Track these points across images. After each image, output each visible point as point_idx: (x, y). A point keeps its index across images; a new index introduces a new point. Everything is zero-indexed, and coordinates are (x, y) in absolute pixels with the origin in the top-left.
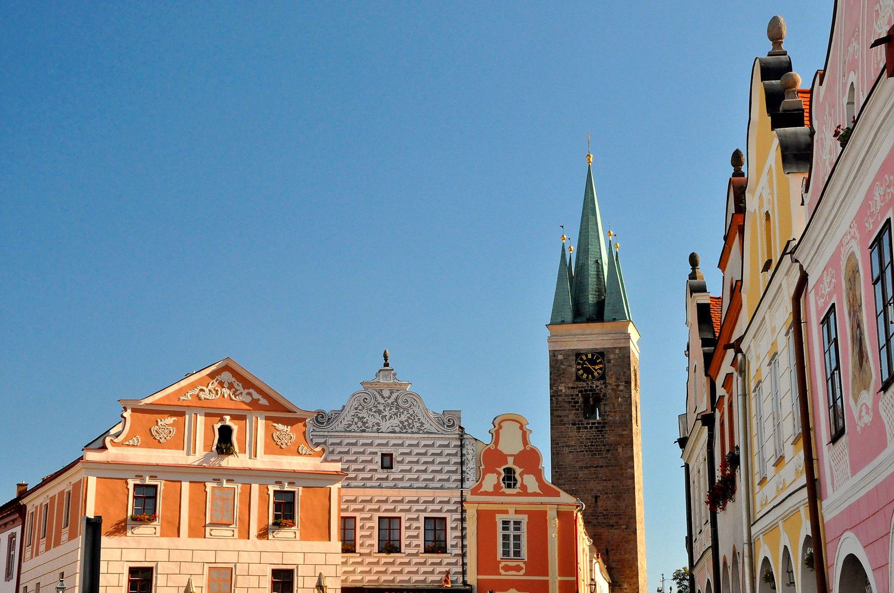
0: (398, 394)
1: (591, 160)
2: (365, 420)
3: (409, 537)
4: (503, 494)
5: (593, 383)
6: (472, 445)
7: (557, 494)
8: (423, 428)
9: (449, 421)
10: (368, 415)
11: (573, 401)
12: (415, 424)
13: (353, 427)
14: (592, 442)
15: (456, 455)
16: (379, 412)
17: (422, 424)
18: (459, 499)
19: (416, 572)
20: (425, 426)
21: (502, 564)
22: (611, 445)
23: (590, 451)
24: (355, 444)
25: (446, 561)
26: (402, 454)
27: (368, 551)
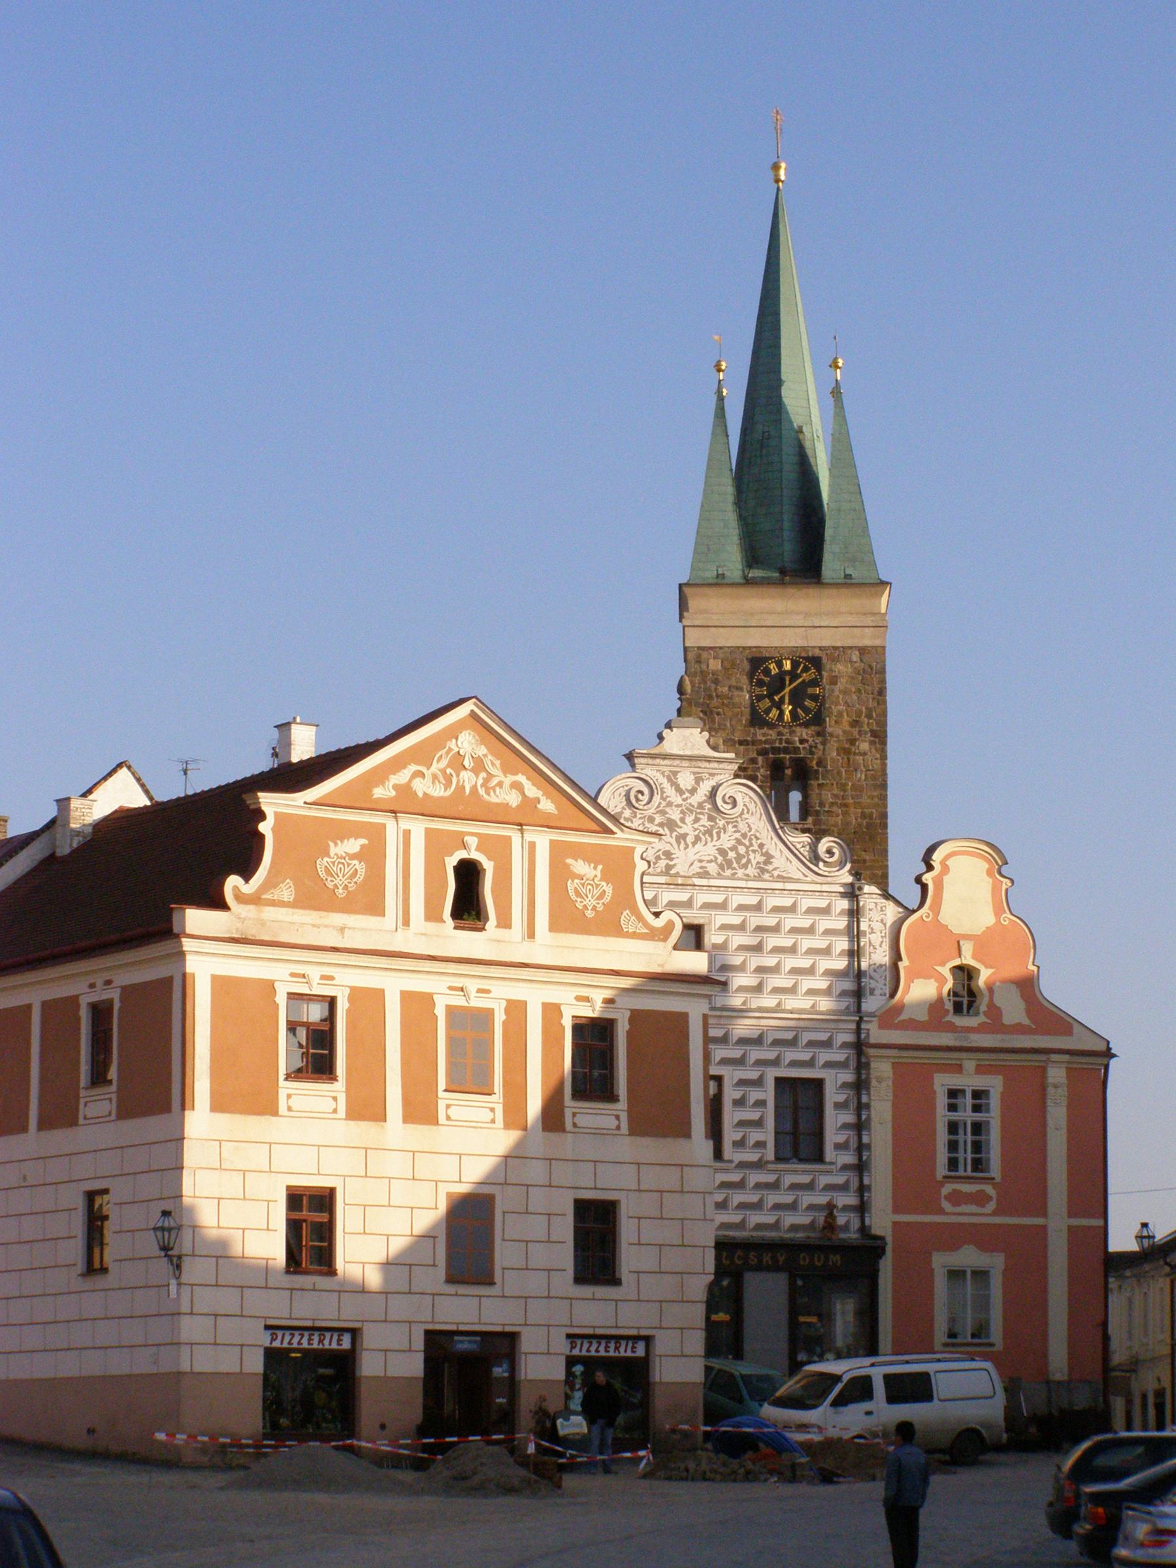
1: (783, 177)
3: (742, 1123)
4: (952, 1028)
6: (882, 911)
8: (770, 868)
12: (752, 856)
16: (671, 825)
17: (769, 858)
20: (776, 863)
21: (947, 1189)
25: (823, 1180)
26: (724, 927)
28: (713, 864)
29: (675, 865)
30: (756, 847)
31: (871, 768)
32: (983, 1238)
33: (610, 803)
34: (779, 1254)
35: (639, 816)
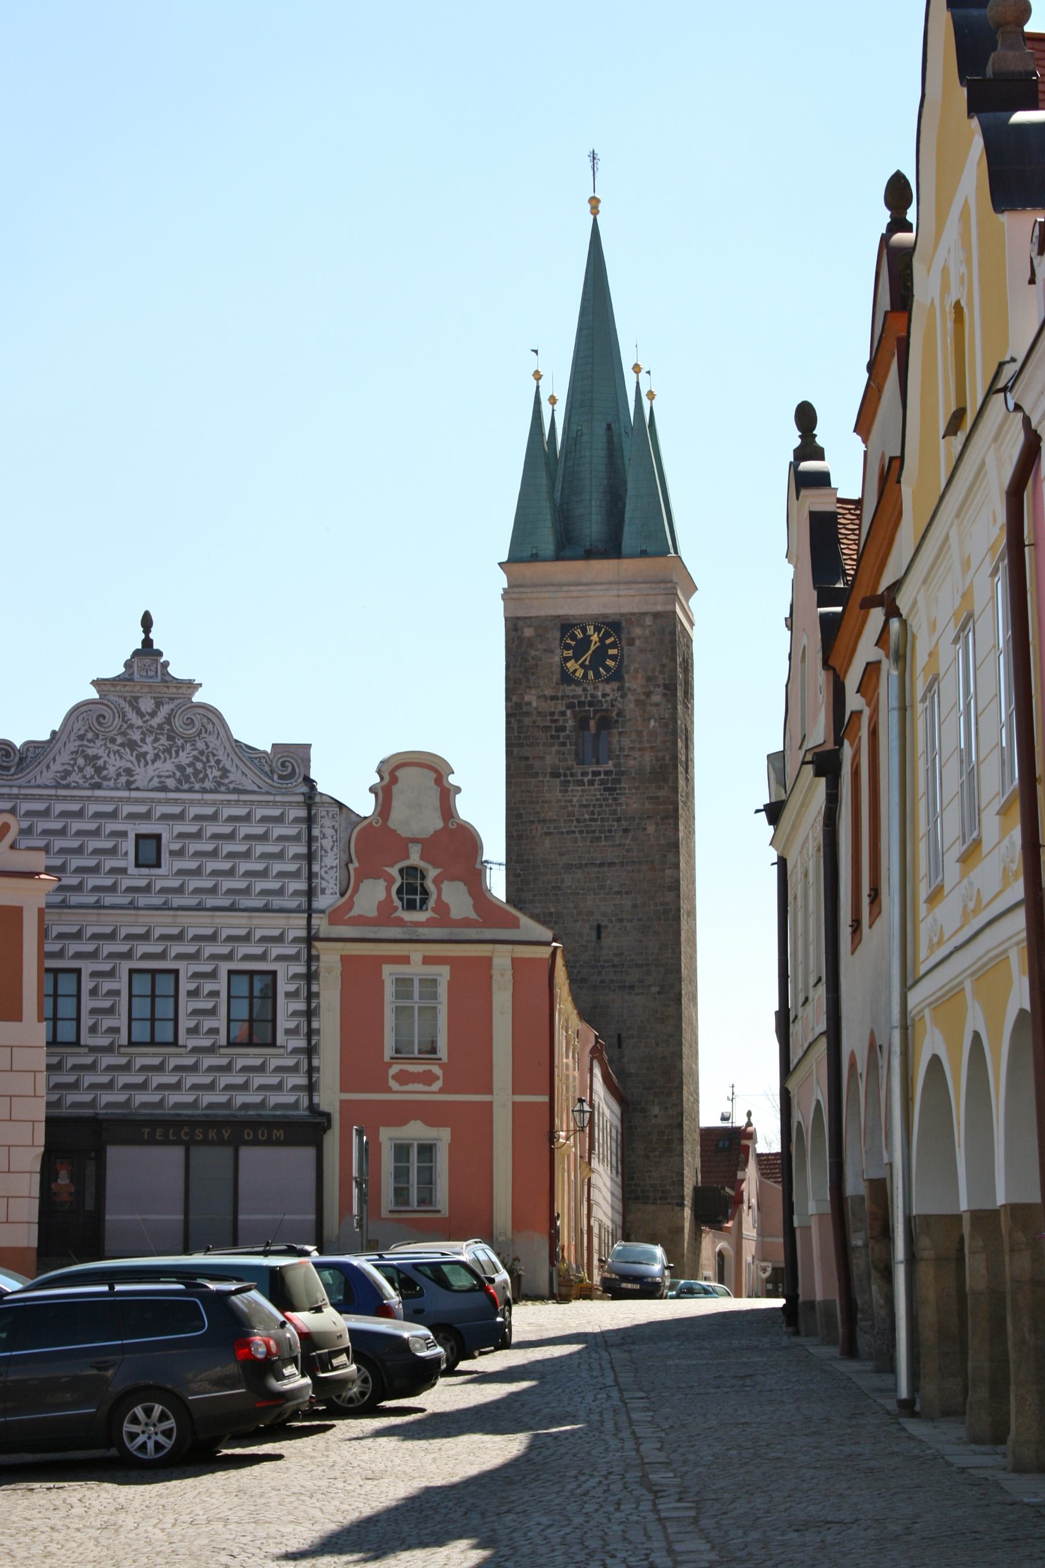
0: (172, 706)
2: (100, 763)
3: (196, 1012)
4: (400, 923)
5: (597, 687)
6: (333, 817)
7: (515, 924)
8: (226, 781)
9: (283, 764)
10: (107, 751)
11: (553, 725)
12: (209, 771)
13: (75, 777)
14: (593, 813)
15: (296, 838)
16: (132, 745)
17: (225, 772)
18: (303, 933)
19: (211, 1087)
20: (232, 777)
21: (395, 1069)
22: (633, 818)
23: (588, 832)
24: (79, 814)
26: (181, 836)
27: (104, 1041)
28: (172, 779)
29: (135, 781)
30: (213, 763)
31: (662, 716)
32: (431, 1114)
33: (74, 726)
34: (224, 1131)
35: (101, 737)
